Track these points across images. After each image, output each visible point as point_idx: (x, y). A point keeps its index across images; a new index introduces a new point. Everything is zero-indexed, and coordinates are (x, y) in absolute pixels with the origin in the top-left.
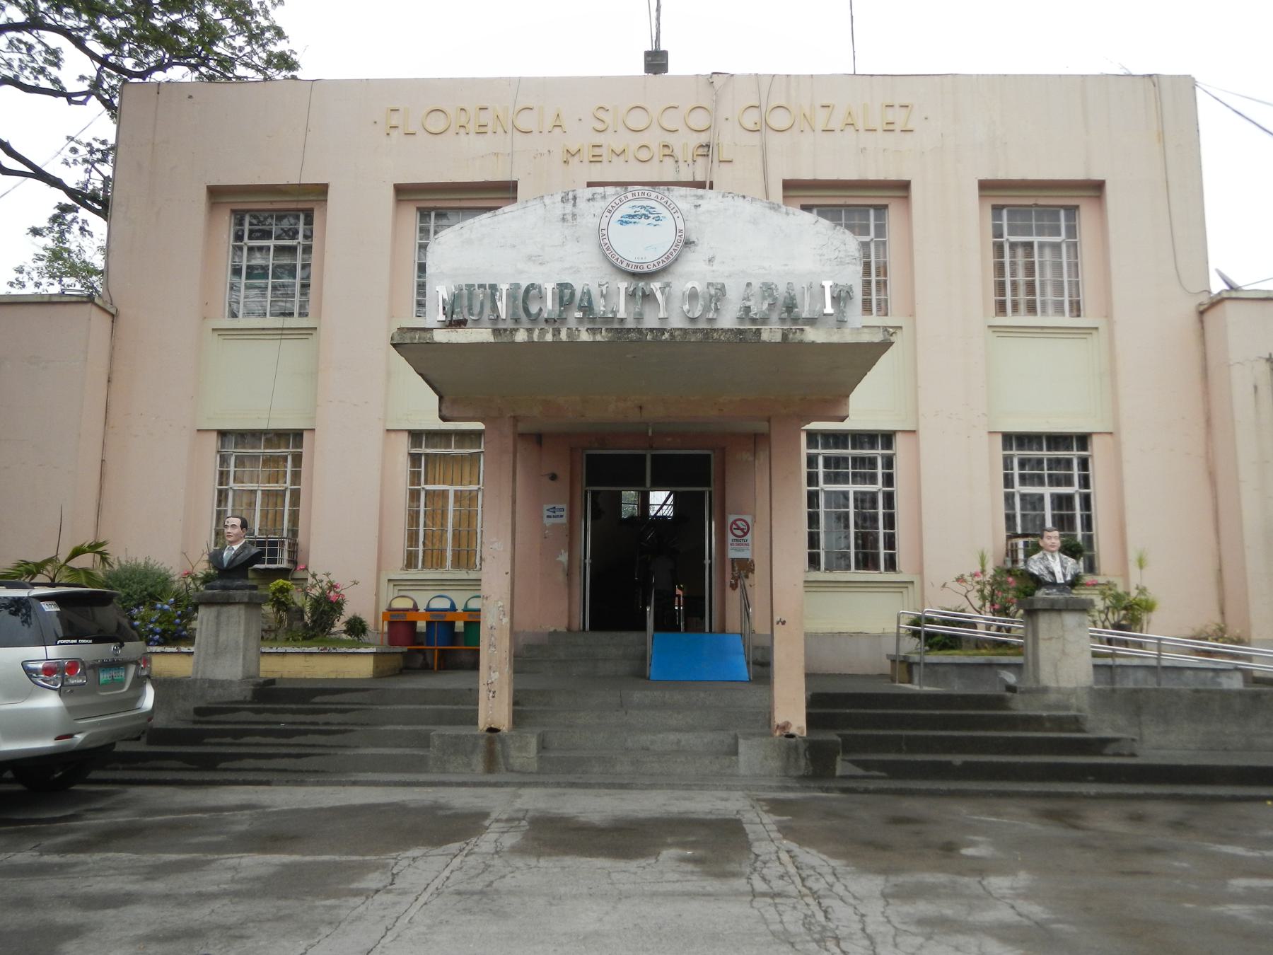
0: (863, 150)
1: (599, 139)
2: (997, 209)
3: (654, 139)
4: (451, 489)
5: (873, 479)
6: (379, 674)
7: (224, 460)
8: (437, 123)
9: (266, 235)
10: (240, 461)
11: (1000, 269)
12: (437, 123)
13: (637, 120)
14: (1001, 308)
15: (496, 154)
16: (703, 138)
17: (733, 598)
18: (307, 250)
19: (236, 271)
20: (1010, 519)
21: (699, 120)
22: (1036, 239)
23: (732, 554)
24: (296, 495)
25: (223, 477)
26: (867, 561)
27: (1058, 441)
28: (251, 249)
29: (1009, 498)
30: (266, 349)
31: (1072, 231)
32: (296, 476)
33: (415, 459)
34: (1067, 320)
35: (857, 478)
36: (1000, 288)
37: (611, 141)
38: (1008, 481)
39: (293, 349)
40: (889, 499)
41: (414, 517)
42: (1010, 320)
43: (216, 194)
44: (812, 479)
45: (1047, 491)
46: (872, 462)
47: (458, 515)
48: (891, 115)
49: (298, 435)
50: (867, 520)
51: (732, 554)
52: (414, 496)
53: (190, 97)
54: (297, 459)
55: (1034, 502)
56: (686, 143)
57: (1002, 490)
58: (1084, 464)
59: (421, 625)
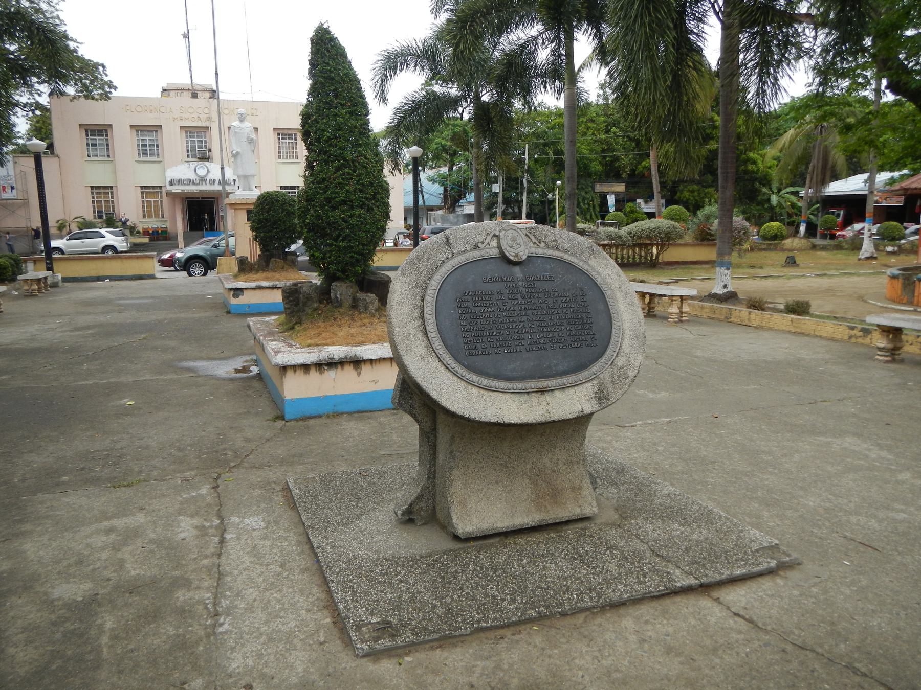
1: (181, 115)
2: (279, 134)
3: (195, 115)
6: (151, 240)
7: (92, 193)
8: (139, 109)
9: (95, 135)
10: (97, 193)
11: (279, 148)
12: (139, 109)
13: (191, 110)
14: (280, 157)
16: (208, 116)
17: (221, 224)
18: (107, 140)
19: (88, 145)
21: (206, 111)
22: (287, 141)
23: (221, 214)
24: (113, 202)
25: (93, 197)
30: (101, 166)
32: (112, 197)
33: (142, 193)
34: (295, 160)
36: (280, 152)
37: (187, 115)
39: (108, 166)
41: (143, 207)
42: (281, 160)
47: (154, 206)
48: (253, 111)
49: (111, 187)
51: (221, 214)
52: (143, 202)
54: (112, 193)
56: (205, 116)
59: (151, 231)
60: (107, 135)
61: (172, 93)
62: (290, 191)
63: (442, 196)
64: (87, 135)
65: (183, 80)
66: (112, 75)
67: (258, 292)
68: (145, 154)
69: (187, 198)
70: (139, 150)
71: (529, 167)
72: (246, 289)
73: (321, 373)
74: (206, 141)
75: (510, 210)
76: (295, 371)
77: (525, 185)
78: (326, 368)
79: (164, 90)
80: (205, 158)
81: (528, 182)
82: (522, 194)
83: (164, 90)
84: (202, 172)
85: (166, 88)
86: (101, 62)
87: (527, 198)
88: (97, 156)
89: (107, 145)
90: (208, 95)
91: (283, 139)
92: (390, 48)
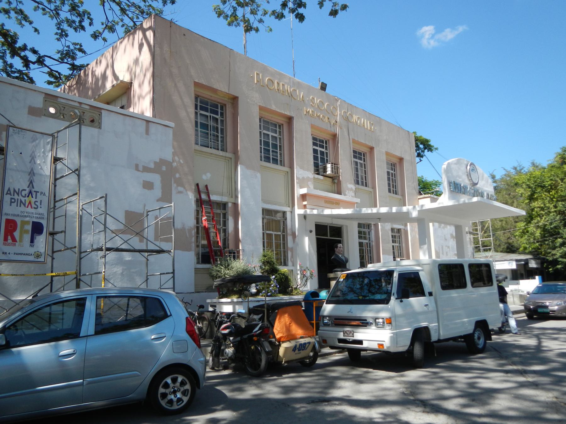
0: (366, 134)
4: (274, 233)
15: (287, 104)
28: (201, 114)
53: (184, 35)
60: (222, 114)
68: (267, 159)
89: (222, 130)
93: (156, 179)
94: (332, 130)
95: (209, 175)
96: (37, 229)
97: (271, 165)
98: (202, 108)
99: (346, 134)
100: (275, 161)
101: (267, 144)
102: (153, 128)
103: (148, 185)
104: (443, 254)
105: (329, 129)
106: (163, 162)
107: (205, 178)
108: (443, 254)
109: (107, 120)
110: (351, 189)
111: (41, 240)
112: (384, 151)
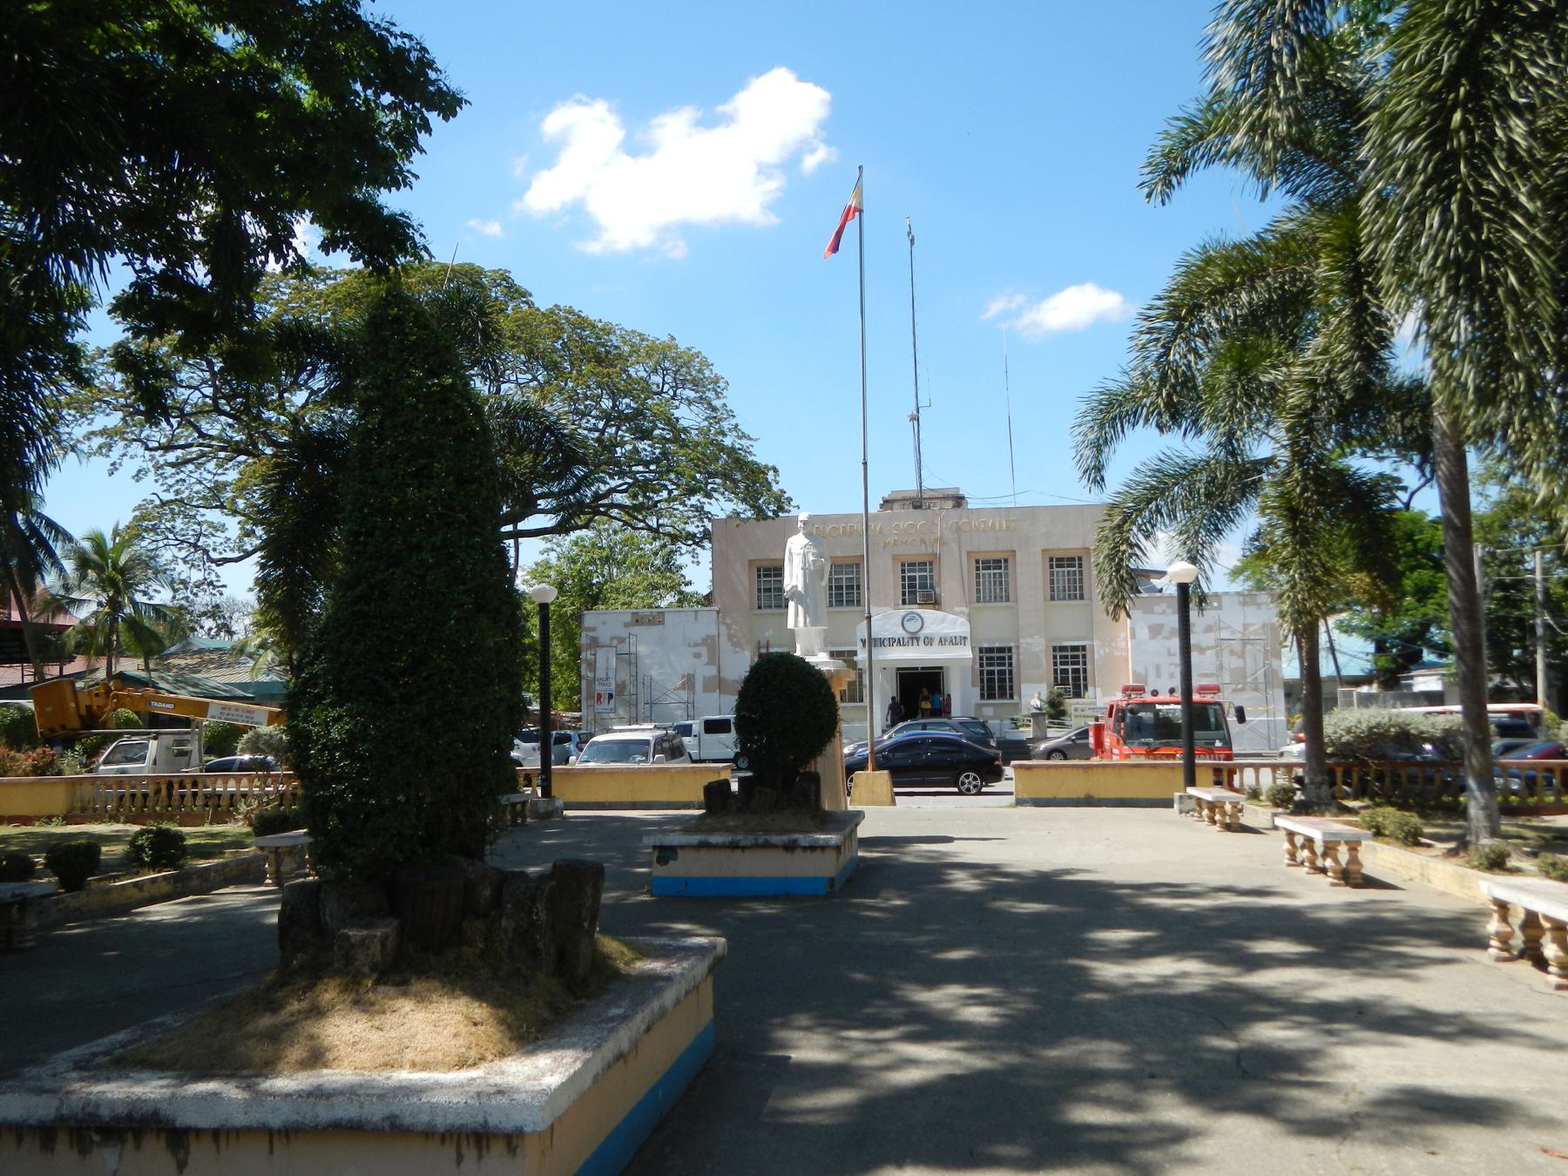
5: (1004, 665)
11: (1052, 582)
19: (759, 590)
20: (1056, 678)
22: (1066, 569)
26: (1003, 696)
27: (1075, 648)
29: (1055, 671)
31: (1080, 566)
35: (999, 665)
38: (1055, 664)
40: (1011, 672)
43: (750, 561)
44: (981, 665)
45: (1070, 667)
46: (1004, 658)
50: (1002, 680)
55: (1065, 671)
57: (1052, 667)
58: (1084, 656)
61: (896, 506)
62: (1069, 653)
63: (1370, 657)
64: (759, 576)
65: (909, 485)
66: (784, 483)
67: (704, 854)
68: (840, 602)
69: (898, 669)
70: (831, 595)
71: (1546, 591)
72: (682, 847)
73: (84, 1149)
74: (932, 578)
75: (1513, 685)
76: (20, 1139)
77: (1540, 631)
78: (96, 1138)
79: (886, 501)
80: (934, 602)
81: (1547, 626)
82: (1535, 652)
83: (886, 501)
84: (913, 626)
85: (886, 496)
86: (770, 465)
87: (1547, 656)
88: (770, 607)
90: (950, 504)
91: (1058, 566)
92: (1113, 386)
93: (703, 650)
94: (930, 550)
95: (771, 632)
96: (611, 696)
97: (845, 609)
98: (765, 576)
99: (956, 548)
100: (850, 602)
101: (839, 588)
102: (700, 615)
103: (698, 656)
104: (1158, 675)
105: (923, 550)
106: (708, 637)
107: (769, 634)
108: (1158, 675)
109: (668, 618)
110: (962, 612)
111: (612, 701)
112: (1039, 550)
